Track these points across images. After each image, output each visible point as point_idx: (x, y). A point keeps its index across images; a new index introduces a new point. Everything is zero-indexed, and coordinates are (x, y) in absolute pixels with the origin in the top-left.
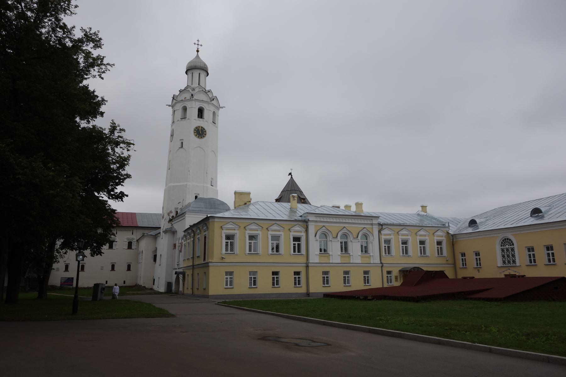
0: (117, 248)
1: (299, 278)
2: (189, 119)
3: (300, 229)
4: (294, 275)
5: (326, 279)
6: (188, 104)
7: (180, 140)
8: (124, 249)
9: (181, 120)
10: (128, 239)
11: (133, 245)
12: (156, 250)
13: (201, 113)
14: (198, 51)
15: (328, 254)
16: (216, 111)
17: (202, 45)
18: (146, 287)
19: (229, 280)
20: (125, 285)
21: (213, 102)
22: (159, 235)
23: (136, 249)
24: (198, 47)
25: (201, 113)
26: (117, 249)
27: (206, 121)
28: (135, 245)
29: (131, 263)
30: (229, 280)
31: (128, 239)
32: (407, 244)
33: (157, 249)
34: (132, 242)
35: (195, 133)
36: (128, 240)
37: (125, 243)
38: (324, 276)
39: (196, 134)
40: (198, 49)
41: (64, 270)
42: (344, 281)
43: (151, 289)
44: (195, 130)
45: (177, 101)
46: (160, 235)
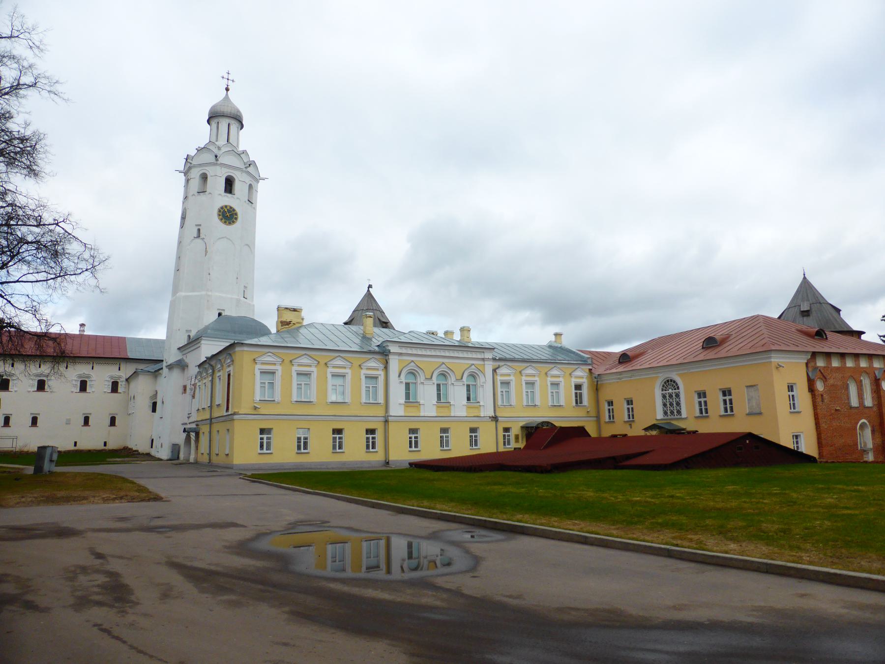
0: (93, 390)
1: (415, 438)
2: (210, 193)
3: (510, 372)
4: (367, 434)
5: (473, 438)
6: (210, 171)
7: (197, 225)
8: (105, 392)
11: (119, 386)
14: (227, 89)
15: (449, 404)
16: (254, 183)
18: (139, 451)
19: (413, 440)
20: (106, 448)
21: (249, 169)
22: (160, 371)
23: (124, 392)
24: (228, 82)
27: (238, 198)
30: (413, 440)
31: (112, 377)
32: (581, 390)
33: (157, 393)
35: (219, 215)
37: (106, 383)
38: (472, 434)
39: (221, 217)
40: (228, 86)
42: (470, 442)
44: (220, 211)
46: (163, 372)
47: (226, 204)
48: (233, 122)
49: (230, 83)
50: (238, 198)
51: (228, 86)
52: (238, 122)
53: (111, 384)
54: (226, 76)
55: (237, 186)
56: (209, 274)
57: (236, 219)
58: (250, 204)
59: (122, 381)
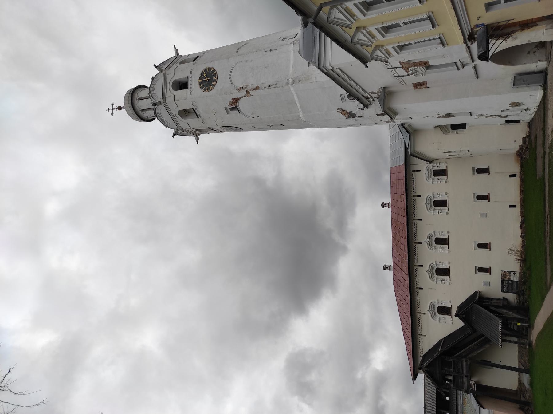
0: (445, 194)
2: (193, 104)
6: (174, 109)
7: (228, 113)
8: (446, 182)
9: (201, 117)
10: (428, 178)
11: (439, 169)
12: (442, 128)
13: (182, 85)
16: (181, 60)
17: (112, 103)
18: (524, 136)
20: (518, 175)
21: (164, 68)
22: (406, 126)
23: (446, 163)
24: (115, 109)
25: (182, 85)
26: (447, 193)
27: (191, 72)
28: (438, 165)
29: (474, 167)
31: (428, 178)
33: (438, 126)
34: (434, 171)
35: (209, 89)
36: (431, 177)
37: (436, 182)
39: (211, 87)
41: (489, 274)
43: (530, 125)
44: (205, 90)
45: (178, 128)
46: (407, 123)
47: (198, 83)
48: (136, 96)
49: (115, 107)
50: (191, 72)
51: (117, 109)
52: (136, 91)
53: (437, 177)
54: (110, 112)
55: (180, 76)
56: (270, 86)
57: (210, 69)
58: (199, 58)
59: (433, 166)
